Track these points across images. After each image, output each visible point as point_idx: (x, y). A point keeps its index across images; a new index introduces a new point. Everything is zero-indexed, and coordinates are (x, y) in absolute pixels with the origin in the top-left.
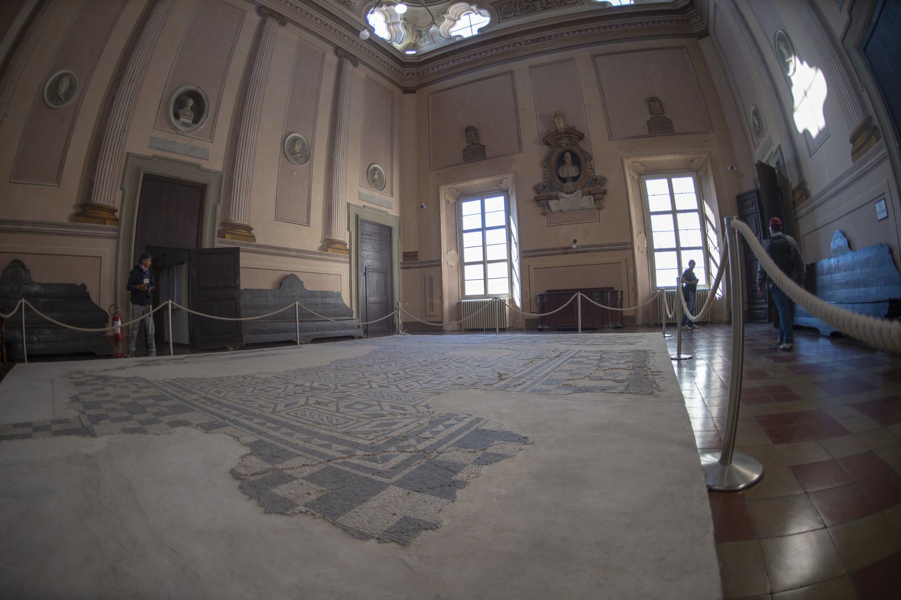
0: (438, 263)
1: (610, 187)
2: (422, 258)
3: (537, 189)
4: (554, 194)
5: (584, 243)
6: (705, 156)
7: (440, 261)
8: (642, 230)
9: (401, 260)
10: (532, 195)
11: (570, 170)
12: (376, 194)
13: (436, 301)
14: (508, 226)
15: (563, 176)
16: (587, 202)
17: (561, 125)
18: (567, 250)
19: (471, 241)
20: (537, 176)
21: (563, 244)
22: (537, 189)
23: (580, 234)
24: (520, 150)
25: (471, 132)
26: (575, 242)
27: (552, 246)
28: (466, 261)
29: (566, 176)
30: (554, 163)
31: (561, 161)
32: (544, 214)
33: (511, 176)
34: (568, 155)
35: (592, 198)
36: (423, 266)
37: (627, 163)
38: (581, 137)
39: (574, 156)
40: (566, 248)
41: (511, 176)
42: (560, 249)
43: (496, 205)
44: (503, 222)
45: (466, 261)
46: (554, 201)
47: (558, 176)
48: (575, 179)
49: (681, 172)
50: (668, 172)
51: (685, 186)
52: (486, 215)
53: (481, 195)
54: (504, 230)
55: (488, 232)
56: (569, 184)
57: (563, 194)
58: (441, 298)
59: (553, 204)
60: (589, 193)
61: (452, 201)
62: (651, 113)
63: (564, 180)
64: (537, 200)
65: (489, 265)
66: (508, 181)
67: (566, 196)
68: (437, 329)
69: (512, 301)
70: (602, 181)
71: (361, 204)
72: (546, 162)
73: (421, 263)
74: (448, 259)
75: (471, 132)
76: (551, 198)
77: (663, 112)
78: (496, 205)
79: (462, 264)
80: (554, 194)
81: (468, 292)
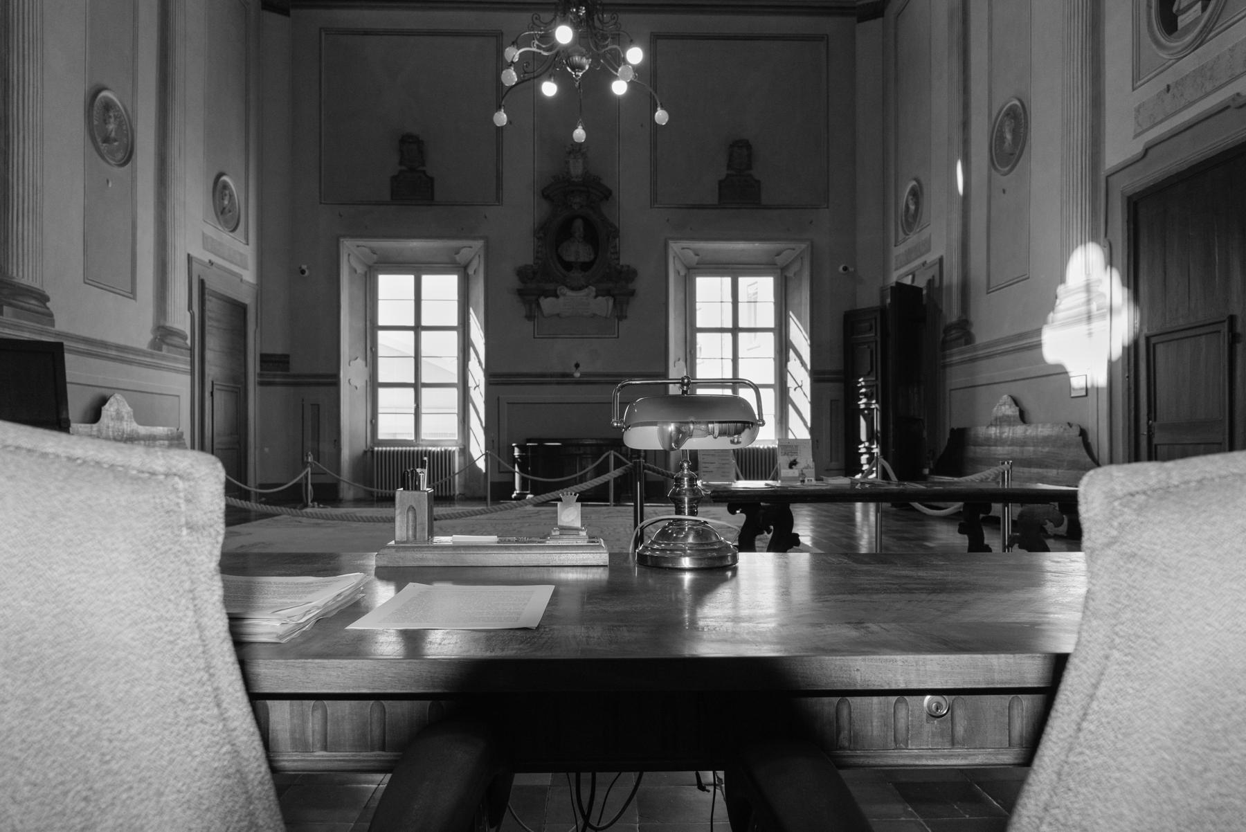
0: (332, 381)
1: (640, 285)
2: (296, 367)
3: (522, 273)
4: (550, 286)
5: (590, 369)
6: (803, 246)
7: (336, 376)
8: (682, 355)
9: (258, 370)
10: (515, 282)
11: (577, 251)
12: (226, 237)
13: (325, 447)
14: (463, 328)
15: (567, 259)
16: (603, 305)
17: (576, 169)
18: (564, 378)
19: (393, 349)
20: (523, 251)
21: (559, 369)
22: (522, 273)
23: (584, 355)
24: (499, 199)
25: (411, 148)
26: (577, 366)
27: (539, 371)
28: (381, 379)
29: (572, 259)
30: (554, 233)
31: (565, 232)
32: (530, 317)
33: (479, 244)
34: (579, 223)
35: (611, 302)
36: (298, 382)
37: (675, 247)
38: (607, 194)
39: (588, 224)
40: (564, 375)
41: (479, 244)
42: (552, 376)
43: (442, 290)
45: (381, 379)
46: (549, 299)
47: (560, 258)
48: (586, 267)
51: (760, 290)
52: (424, 304)
53: (417, 267)
54: (454, 334)
55: (424, 334)
56: (576, 275)
57: (566, 290)
58: (337, 442)
59: (547, 304)
60: (608, 293)
61: (360, 270)
62: (729, 167)
63: (568, 266)
64: (521, 293)
65: (424, 391)
66: (472, 249)
67: (570, 293)
68: (328, 494)
69: (465, 450)
70: (629, 275)
71: (206, 256)
72: (541, 231)
73: (294, 376)
74: (351, 374)
75: (411, 148)
76: (547, 294)
77: (750, 167)
78: (442, 290)
79: (374, 385)
80: (550, 286)
81: (383, 434)
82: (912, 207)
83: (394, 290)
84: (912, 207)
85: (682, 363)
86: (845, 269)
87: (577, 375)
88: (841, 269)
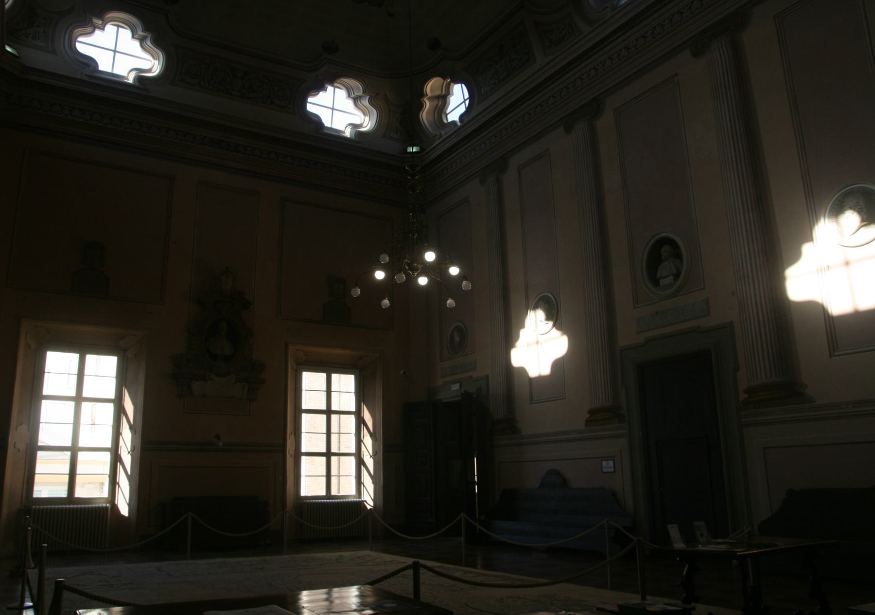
43: (103, 368)
44: (112, 395)
49: (343, 369)
50: (329, 366)
51: (345, 385)
52: (86, 379)
53: (83, 346)
78: (103, 368)
82: (457, 339)
83: (59, 367)
84: (457, 339)
85: (293, 436)
86: (404, 373)
87: (221, 444)
88: (402, 372)
